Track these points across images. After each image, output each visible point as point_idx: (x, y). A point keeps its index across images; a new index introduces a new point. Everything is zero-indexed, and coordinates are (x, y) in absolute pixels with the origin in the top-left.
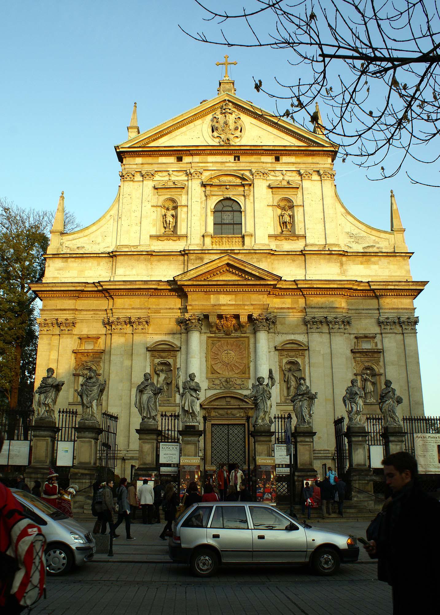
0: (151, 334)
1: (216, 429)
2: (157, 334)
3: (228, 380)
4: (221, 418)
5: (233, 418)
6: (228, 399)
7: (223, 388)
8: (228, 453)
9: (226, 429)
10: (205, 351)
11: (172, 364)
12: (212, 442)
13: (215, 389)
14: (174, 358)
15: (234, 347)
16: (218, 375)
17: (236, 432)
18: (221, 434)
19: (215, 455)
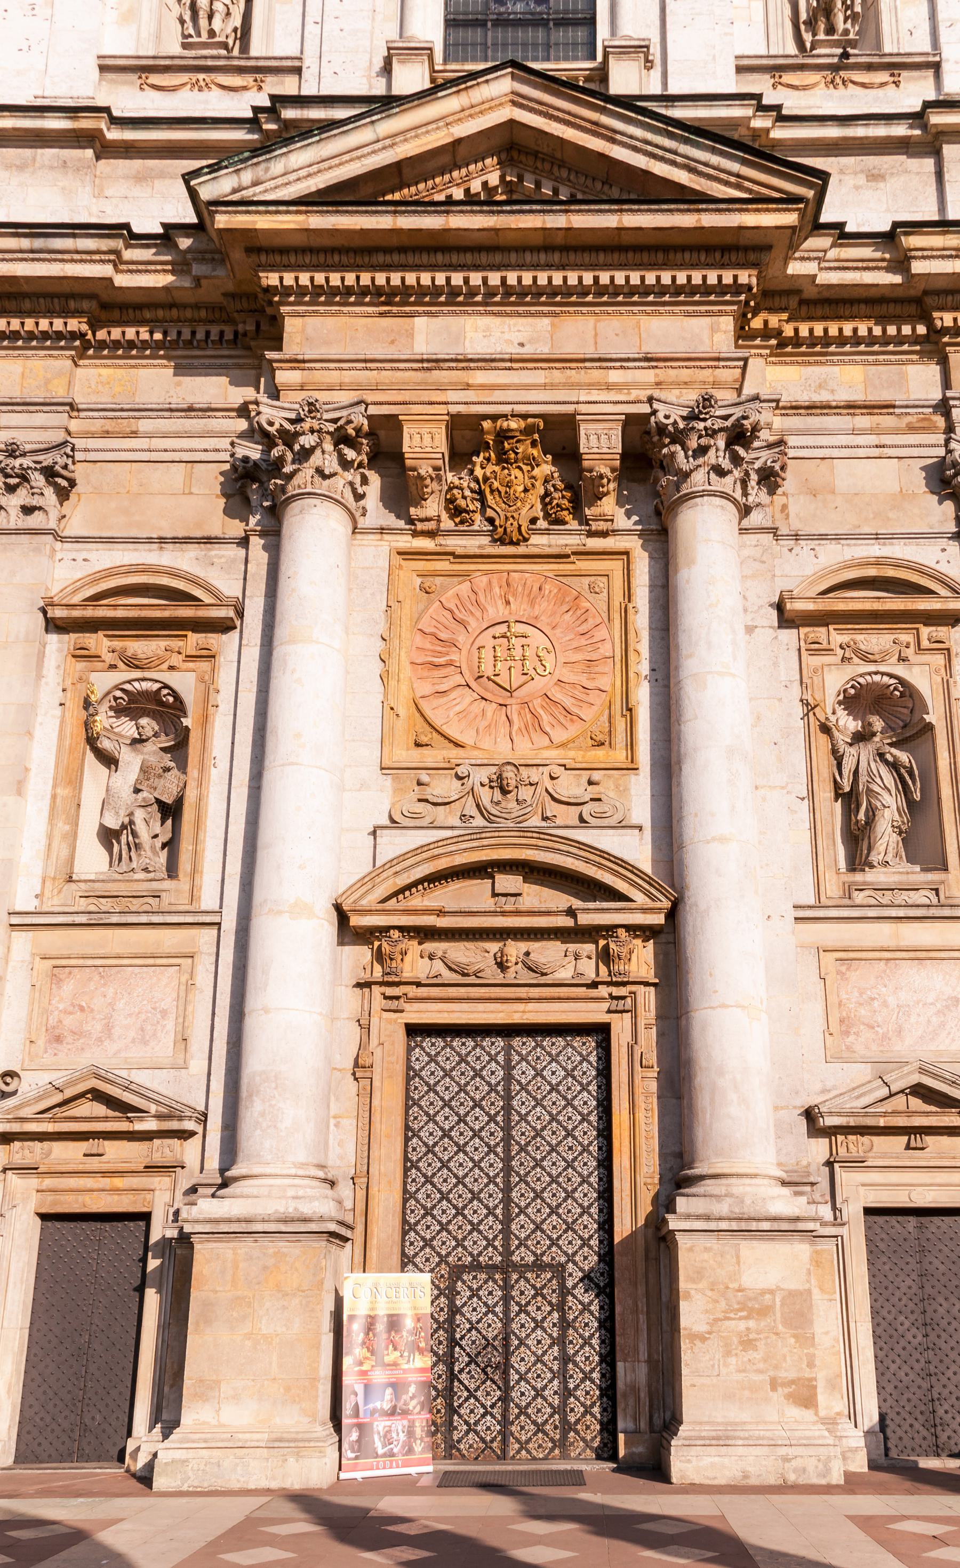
0: (78, 540)
1: (432, 1059)
2: (111, 540)
3: (509, 773)
4: (462, 991)
5: (535, 992)
6: (507, 882)
7: (479, 821)
8: (507, 1201)
9: (493, 1059)
10: (382, 628)
11: (190, 698)
12: (409, 1133)
13: (432, 827)
14: (204, 666)
15: (542, 607)
16: (454, 753)
17: (554, 1073)
18: (462, 1089)
19: (428, 1212)
